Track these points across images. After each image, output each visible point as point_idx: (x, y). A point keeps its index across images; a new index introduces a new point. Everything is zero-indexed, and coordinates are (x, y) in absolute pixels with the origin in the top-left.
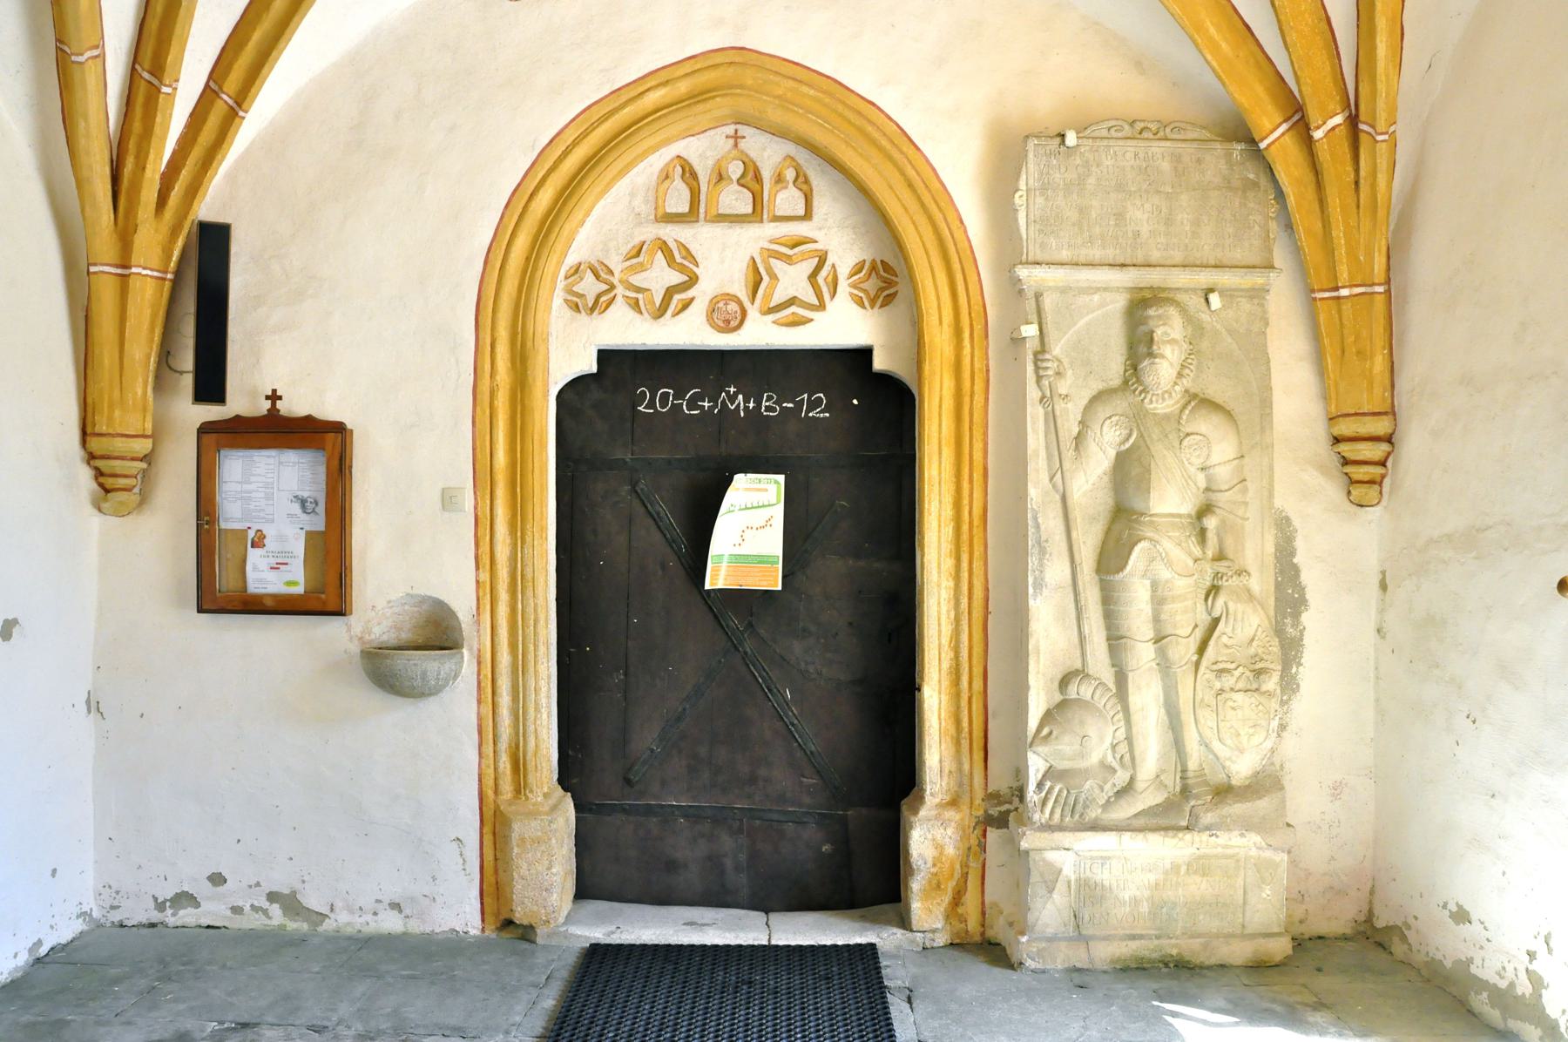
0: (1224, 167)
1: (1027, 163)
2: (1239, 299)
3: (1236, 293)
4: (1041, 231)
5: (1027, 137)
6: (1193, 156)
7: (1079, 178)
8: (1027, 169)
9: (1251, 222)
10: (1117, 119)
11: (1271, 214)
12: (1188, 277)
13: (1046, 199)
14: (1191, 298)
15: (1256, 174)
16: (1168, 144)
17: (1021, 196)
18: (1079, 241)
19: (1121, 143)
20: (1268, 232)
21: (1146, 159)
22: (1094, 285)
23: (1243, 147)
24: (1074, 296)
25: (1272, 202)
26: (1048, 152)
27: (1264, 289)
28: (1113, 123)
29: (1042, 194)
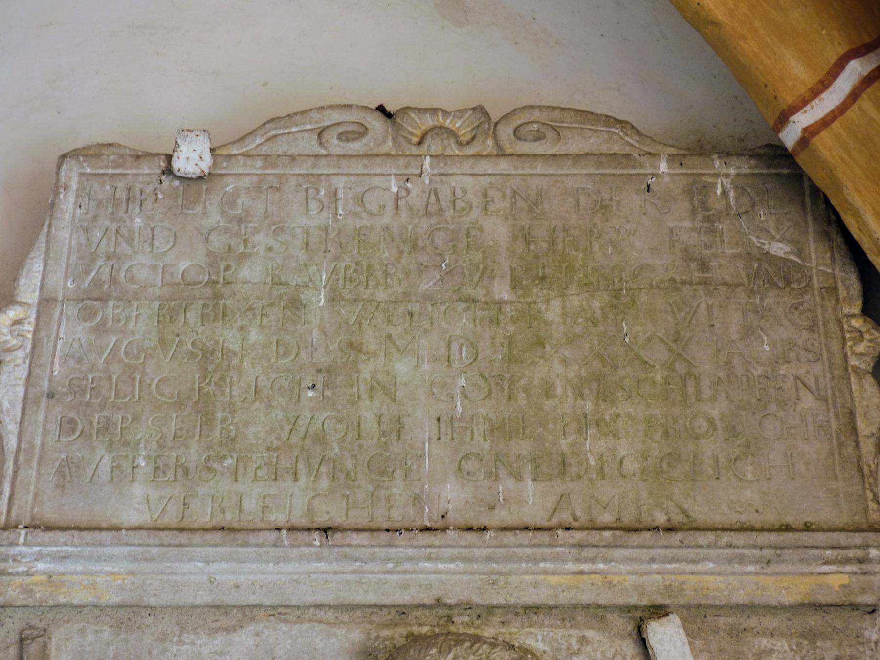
0: (687, 224)
1: (50, 226)
2: (765, 643)
3: (753, 622)
4: (68, 426)
5: (64, 157)
6: (582, 198)
7: (213, 264)
8: (48, 242)
9: (789, 383)
10: (349, 106)
11: (853, 362)
12: (571, 566)
13: (100, 329)
14: (583, 640)
15: (791, 241)
16: (504, 166)
17: (18, 322)
18: (194, 454)
19: (357, 167)
20: (852, 413)
21: (433, 208)
22: (232, 598)
23: (746, 170)
24: (163, 638)
25: (857, 323)
26: (122, 194)
27: (854, 607)
28: (337, 116)
29: (86, 315)
